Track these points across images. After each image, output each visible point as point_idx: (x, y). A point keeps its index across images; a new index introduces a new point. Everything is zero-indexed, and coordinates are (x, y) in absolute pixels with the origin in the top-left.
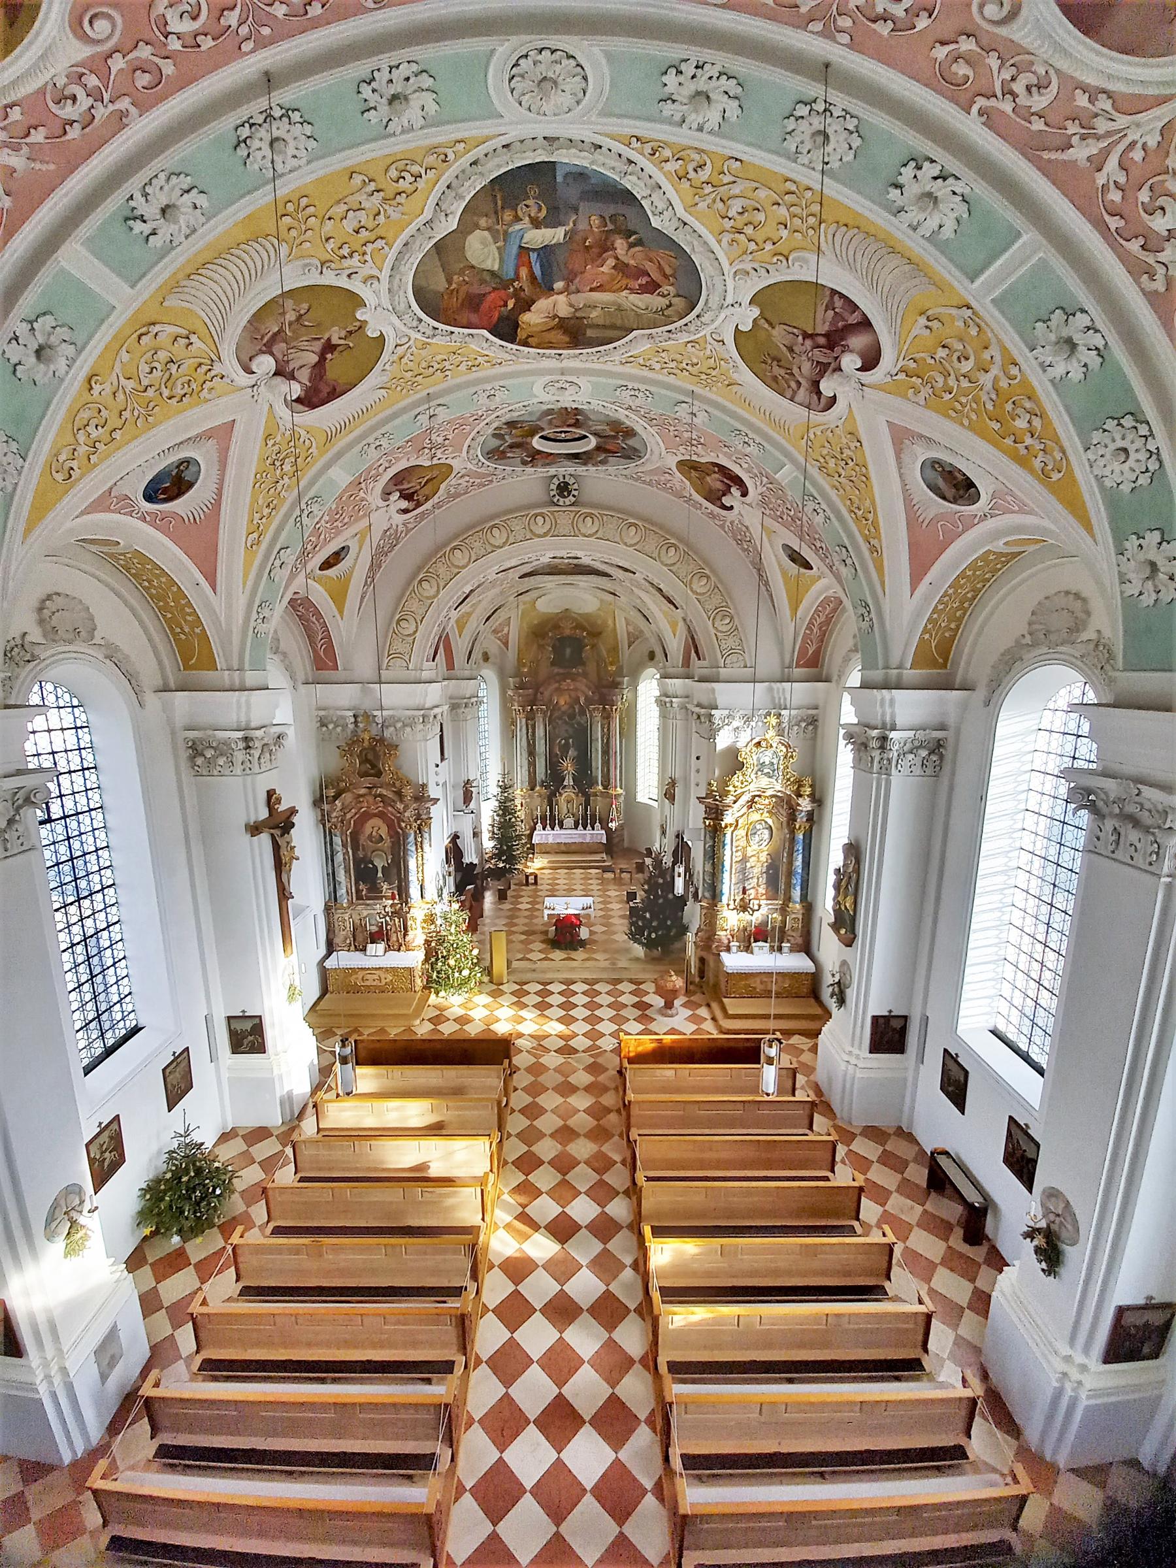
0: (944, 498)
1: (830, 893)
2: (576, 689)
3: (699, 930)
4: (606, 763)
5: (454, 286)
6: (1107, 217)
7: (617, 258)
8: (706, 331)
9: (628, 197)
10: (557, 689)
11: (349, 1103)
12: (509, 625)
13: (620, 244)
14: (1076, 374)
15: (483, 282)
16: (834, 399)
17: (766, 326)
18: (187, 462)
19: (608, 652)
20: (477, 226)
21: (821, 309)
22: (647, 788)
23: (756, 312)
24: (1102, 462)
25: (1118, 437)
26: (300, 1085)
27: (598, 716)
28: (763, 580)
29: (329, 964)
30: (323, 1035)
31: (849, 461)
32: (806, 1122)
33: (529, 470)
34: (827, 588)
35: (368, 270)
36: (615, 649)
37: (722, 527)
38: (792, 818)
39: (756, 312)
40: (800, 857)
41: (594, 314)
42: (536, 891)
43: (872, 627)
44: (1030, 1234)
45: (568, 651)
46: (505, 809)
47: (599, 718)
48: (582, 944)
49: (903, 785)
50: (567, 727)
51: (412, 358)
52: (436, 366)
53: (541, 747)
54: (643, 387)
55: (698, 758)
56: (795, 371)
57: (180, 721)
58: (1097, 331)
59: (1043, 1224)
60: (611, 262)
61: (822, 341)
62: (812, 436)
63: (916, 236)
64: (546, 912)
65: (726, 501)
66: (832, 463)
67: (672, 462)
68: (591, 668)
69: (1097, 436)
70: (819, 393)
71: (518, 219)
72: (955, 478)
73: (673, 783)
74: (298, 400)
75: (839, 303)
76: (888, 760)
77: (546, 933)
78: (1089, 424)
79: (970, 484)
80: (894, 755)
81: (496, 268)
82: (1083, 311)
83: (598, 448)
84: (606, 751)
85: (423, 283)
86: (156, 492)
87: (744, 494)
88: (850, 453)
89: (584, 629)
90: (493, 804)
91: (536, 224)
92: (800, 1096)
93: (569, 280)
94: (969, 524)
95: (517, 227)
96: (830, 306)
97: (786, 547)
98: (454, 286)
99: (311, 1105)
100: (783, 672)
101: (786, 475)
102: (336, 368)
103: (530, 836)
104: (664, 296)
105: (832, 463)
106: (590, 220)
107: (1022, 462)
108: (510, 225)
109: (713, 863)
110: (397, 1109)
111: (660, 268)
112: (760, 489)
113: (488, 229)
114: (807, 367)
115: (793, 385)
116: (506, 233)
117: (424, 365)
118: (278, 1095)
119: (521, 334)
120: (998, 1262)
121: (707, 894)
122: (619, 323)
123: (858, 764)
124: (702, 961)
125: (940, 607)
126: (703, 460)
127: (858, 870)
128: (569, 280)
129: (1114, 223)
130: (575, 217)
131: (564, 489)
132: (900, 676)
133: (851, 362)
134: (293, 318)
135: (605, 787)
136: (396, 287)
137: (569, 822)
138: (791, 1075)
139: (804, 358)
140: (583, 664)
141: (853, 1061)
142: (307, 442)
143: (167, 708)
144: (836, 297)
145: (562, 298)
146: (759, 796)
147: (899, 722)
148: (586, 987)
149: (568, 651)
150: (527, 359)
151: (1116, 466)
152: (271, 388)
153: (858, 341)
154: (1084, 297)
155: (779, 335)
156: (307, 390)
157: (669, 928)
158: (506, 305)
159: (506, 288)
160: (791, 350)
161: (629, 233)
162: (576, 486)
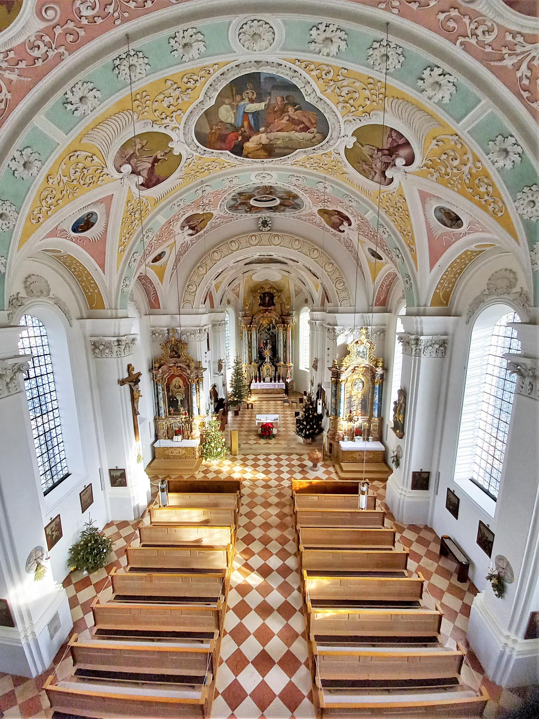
0: (446, 225)
1: (392, 413)
2: (271, 317)
3: (329, 430)
4: (285, 352)
6: (522, 92)
7: (289, 116)
8: (331, 149)
9: (294, 88)
11: (165, 510)
13: (291, 109)
14: (509, 166)
15: (227, 128)
16: (392, 180)
17: (360, 146)
18: (92, 214)
19: (286, 299)
20: (224, 103)
21: (386, 137)
22: (304, 363)
23: (355, 139)
24: (522, 207)
25: (530, 195)
26: (142, 501)
27: (281, 330)
28: (359, 265)
29: (156, 445)
30: (153, 478)
31: (400, 208)
32: (381, 522)
33: (249, 215)
34: (390, 269)
35: (173, 125)
36: (289, 298)
37: (339, 240)
38: (373, 377)
39: (355, 139)
40: (377, 396)
41: (279, 142)
42: (253, 411)
43: (411, 287)
44: (490, 578)
45: (267, 299)
46: (238, 373)
47: (281, 330)
48: (274, 436)
49: (426, 362)
50: (267, 335)
51: (194, 164)
52: (205, 168)
53: (254, 344)
54: (302, 175)
55: (328, 349)
56: (374, 166)
57: (88, 333)
58: (518, 145)
59: (496, 573)
60: (287, 118)
61: (386, 152)
62: (382, 197)
63: (431, 102)
64: (257, 421)
65: (341, 228)
66: (391, 210)
67: (315, 210)
68: (278, 306)
69: (519, 195)
70: (385, 177)
71: (243, 99)
72: (451, 216)
73: (316, 361)
74: (142, 185)
75: (394, 134)
76: (419, 350)
77: (257, 431)
78: (515, 189)
79: (458, 219)
80: (422, 347)
81: (233, 122)
82: (512, 136)
83: (281, 204)
84: (285, 346)
85: (199, 130)
86: (77, 228)
87: (350, 225)
88: (400, 205)
89: (275, 289)
90: (232, 371)
91: (252, 101)
92: (378, 510)
93: (267, 127)
94: (458, 237)
95: (242, 103)
96: (390, 136)
97: (370, 249)
98: (214, 131)
99: (147, 511)
100: (369, 309)
101: (370, 215)
102: (159, 170)
103: (250, 386)
105: (391, 210)
106: (277, 99)
107: (484, 208)
108: (239, 102)
109: (336, 399)
110: (187, 513)
111: (310, 120)
112: (357, 222)
113: (229, 104)
114: (379, 164)
115: (373, 173)
116: (237, 106)
117: (200, 167)
118: (133, 506)
119: (245, 152)
120: (474, 591)
121: (333, 413)
122: (290, 146)
123: (405, 351)
124: (331, 445)
125: (444, 277)
126: (330, 209)
127: (405, 402)
128: (267, 127)
129: (525, 95)
130: (269, 98)
131: (265, 223)
132: (425, 310)
133: (400, 162)
134: (140, 147)
135: (285, 363)
136: (187, 133)
137: (268, 379)
138: (373, 499)
139: (378, 160)
140: (274, 305)
141: (404, 493)
142: (146, 204)
143: (82, 327)
144: (393, 132)
145: (263, 135)
146: (358, 367)
147: (425, 331)
148: (276, 457)
149: (267, 299)
150: (247, 163)
151: (529, 209)
152: (130, 180)
153: (403, 152)
154: (511, 129)
155: (366, 150)
156: (146, 180)
157: (315, 429)
160: (371, 157)
161: (294, 105)
162: (270, 222)
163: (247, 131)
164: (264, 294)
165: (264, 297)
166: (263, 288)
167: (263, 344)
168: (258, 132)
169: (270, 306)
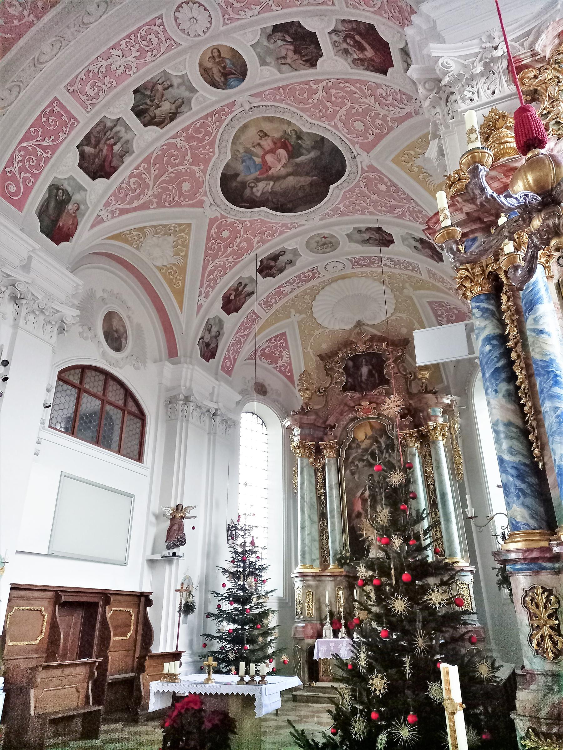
10: (352, 420)
12: (287, 347)
27: (415, 448)
45: (365, 370)
47: (415, 451)
109: (514, 396)
140: (387, 382)
149: (365, 370)
164: (355, 359)
165: (357, 367)
166: (352, 343)
167: (364, 501)
169: (375, 387)
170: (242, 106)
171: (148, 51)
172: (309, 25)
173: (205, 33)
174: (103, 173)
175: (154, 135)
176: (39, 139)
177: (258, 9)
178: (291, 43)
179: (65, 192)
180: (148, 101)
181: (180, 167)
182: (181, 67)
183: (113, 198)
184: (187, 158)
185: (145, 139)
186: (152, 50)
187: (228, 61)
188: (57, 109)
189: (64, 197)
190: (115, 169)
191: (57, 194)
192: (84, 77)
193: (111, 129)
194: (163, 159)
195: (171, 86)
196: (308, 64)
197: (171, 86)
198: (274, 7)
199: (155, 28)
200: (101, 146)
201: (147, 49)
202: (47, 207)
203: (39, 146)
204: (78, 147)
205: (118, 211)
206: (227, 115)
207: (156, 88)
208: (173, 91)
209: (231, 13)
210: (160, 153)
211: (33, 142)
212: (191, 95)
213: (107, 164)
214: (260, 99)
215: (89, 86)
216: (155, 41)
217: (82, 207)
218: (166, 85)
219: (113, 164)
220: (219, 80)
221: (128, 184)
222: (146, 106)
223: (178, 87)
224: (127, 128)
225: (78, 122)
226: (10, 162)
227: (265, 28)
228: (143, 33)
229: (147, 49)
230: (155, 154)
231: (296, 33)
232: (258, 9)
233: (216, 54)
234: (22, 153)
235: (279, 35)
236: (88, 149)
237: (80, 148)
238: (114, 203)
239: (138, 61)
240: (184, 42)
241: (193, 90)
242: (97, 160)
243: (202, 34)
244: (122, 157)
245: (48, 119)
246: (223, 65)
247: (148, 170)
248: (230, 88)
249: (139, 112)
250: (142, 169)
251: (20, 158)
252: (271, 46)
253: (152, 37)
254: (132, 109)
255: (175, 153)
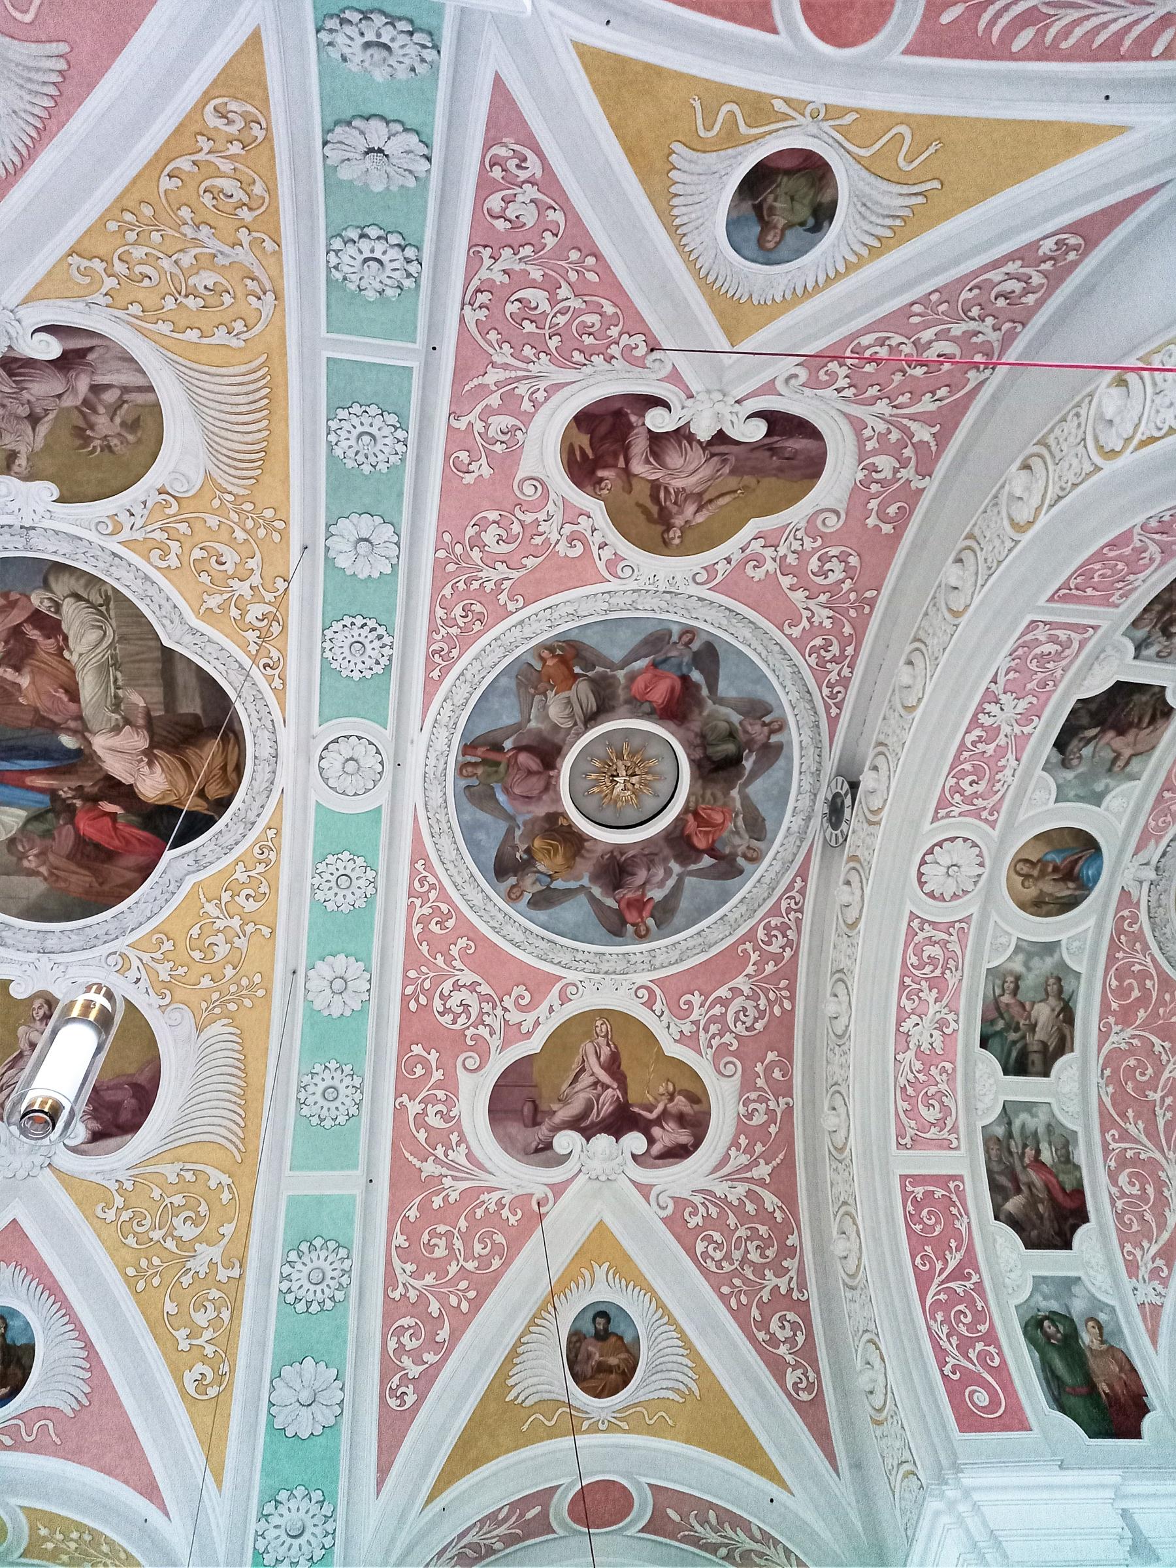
5: (43, 870)
65: (757, 431)
81: (23, 814)
93: (56, 727)
98: (43, 870)
104: (58, 607)
126: (595, 507)
128: (56, 727)
145: (100, 743)
158: (113, 816)
159: (71, 810)
163: (75, 784)
168: (83, 758)
170: (1141, 882)
171: (943, 973)
172: (1097, 685)
173: (981, 865)
174: (1071, 1221)
175: (1074, 1072)
176: (939, 1266)
177: (1011, 756)
178: (1103, 731)
179: (1053, 1316)
180: (1013, 1036)
181: (1166, 1075)
182: (1003, 940)
183: (1128, 1247)
184: (1158, 1049)
185: (1067, 1093)
186: (945, 967)
187: (1049, 857)
188: (919, 1191)
189: (1061, 1328)
190: (1079, 1192)
191: (1048, 1337)
192: (906, 1106)
193: (1010, 1135)
194: (1126, 1097)
195: (1018, 978)
196: (1160, 722)
197: (1018, 978)
198: (1026, 730)
199: (921, 936)
200: (1023, 1178)
201: (938, 972)
202: (1053, 1372)
203: (948, 1279)
204: (996, 1218)
205: (1160, 1262)
206: (1135, 919)
207: (1002, 1006)
208: (1030, 981)
209: (985, 803)
210: (1111, 1089)
211: (936, 1281)
212: (1056, 956)
213: (1060, 1197)
214: (1153, 842)
215: (923, 1110)
216: (935, 951)
217: (1102, 1317)
218: (1010, 986)
219: (1068, 1188)
220: (1068, 892)
221: (1123, 1194)
222: (1019, 1046)
223: (1029, 969)
224: (1029, 1107)
225: (960, 1178)
226: (941, 1355)
227: (1047, 762)
228: (914, 960)
229: (938, 972)
230: (1107, 1101)
231: (1092, 715)
232: (1011, 756)
233: (1027, 868)
234: (940, 1316)
235: (1074, 744)
236: (1013, 1205)
237: (1002, 1217)
238: (1138, 1253)
239: (944, 1002)
240: (970, 907)
241: (1051, 948)
242: (1041, 1208)
243: (980, 870)
244: (1066, 1159)
245: (921, 1221)
246: (1050, 869)
247: (1125, 1136)
248: (1095, 882)
249: (1018, 1066)
250: (1113, 1145)
251: (945, 1329)
252: (1081, 770)
253: (929, 950)
254: (1006, 1073)
255: (1132, 1063)
